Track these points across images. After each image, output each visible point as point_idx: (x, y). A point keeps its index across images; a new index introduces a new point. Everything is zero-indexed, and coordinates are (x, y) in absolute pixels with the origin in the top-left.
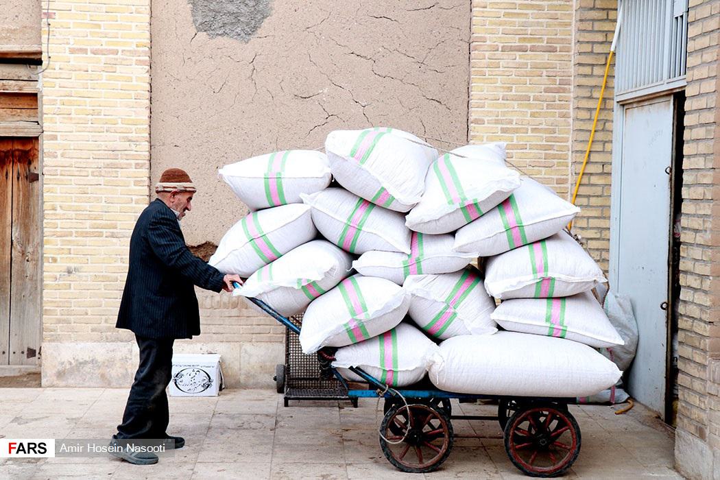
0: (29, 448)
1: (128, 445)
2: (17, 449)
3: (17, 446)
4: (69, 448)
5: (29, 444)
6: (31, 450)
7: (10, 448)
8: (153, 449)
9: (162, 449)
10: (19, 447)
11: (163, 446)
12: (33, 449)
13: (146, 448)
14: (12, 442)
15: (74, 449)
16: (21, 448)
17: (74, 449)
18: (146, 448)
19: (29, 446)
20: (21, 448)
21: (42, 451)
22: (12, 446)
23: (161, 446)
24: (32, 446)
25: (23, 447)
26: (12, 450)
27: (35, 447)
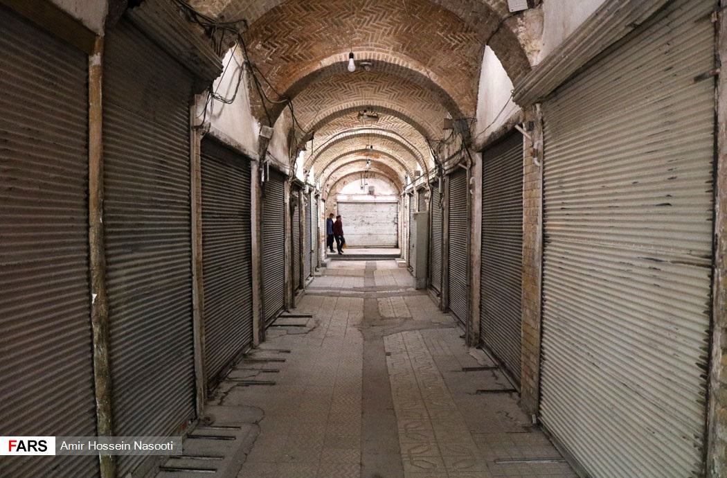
0: (29, 446)
1: (135, 443)
3: (17, 444)
5: (29, 442)
7: (10, 446)
8: (161, 447)
9: (170, 448)
10: (20, 444)
11: (170, 443)
14: (12, 440)
15: (75, 446)
16: (21, 446)
17: (75, 446)
19: (29, 443)
20: (21, 446)
21: (43, 448)
22: (12, 443)
23: (168, 444)
24: (32, 444)
25: (23, 445)
27: (36, 445)
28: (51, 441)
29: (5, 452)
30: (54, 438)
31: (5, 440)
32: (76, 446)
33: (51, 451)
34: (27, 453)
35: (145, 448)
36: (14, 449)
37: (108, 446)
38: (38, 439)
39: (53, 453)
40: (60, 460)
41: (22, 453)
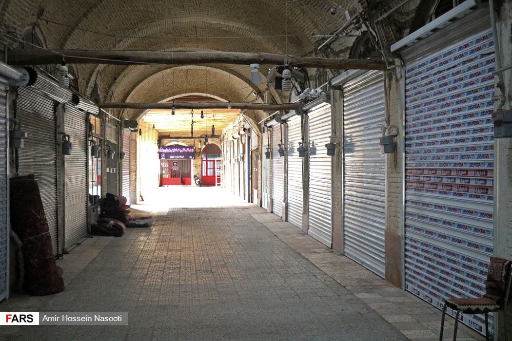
0: (21, 318)
1: (95, 316)
2: (12, 319)
3: (12, 317)
4: (49, 318)
5: (21, 315)
6: (22, 320)
7: (7, 318)
8: (113, 319)
9: (120, 319)
10: (14, 317)
11: (120, 317)
12: (23, 319)
13: (108, 319)
15: (53, 319)
16: (15, 318)
17: (53, 319)
18: (108, 319)
19: (20, 317)
20: (15, 318)
21: (30, 320)
22: (9, 317)
23: (119, 317)
24: (23, 317)
25: (16, 318)
26: (9, 320)
27: (25, 318)
28: (36, 315)
29: (4, 323)
30: (38, 313)
31: (4, 314)
32: (52, 319)
33: (36, 322)
34: (19, 324)
35: (102, 320)
36: (10, 321)
37: (76, 319)
38: (27, 313)
39: (38, 324)
40: (42, 327)
41: (15, 323)
